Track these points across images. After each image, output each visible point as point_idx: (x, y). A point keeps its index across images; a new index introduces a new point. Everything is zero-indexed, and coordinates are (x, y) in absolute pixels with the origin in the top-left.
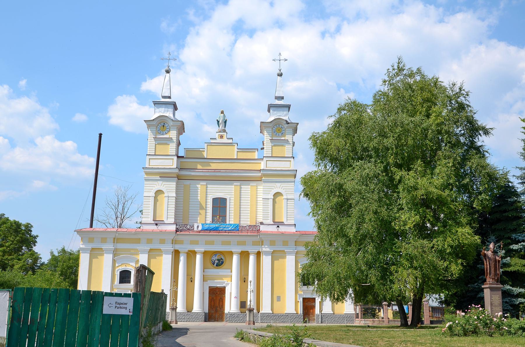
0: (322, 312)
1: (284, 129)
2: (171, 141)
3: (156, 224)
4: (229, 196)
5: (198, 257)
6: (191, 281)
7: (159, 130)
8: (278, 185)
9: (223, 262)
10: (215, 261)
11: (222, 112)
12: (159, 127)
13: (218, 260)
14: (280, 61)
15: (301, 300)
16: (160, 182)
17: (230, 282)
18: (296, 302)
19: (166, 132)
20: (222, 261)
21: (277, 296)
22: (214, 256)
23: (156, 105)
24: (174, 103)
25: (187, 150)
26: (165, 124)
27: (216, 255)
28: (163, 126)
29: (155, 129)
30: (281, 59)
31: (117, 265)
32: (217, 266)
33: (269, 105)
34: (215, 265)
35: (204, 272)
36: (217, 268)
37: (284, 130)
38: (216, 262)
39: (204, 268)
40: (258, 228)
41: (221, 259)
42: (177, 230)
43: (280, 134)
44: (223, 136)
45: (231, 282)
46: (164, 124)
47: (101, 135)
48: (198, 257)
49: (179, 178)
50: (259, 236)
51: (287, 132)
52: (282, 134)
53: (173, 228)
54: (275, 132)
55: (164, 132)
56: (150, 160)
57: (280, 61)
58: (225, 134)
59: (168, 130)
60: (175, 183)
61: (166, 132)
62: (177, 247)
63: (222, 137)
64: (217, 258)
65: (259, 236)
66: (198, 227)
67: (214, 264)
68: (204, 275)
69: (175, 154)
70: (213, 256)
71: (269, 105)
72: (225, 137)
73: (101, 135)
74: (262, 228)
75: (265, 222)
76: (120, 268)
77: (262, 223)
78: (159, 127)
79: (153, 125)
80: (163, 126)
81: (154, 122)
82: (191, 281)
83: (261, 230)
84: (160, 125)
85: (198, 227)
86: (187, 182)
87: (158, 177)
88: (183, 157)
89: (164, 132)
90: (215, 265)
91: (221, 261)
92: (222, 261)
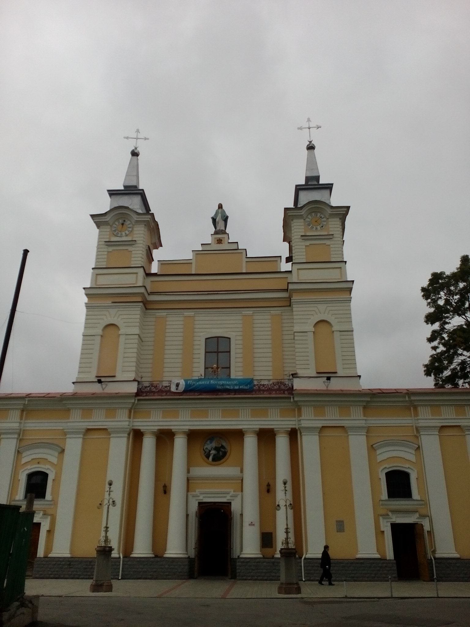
0: (437, 556)
1: (325, 219)
2: (134, 246)
3: (100, 381)
4: (234, 334)
5: (180, 443)
6: (165, 492)
7: (115, 231)
8: (322, 307)
9: (225, 454)
10: (210, 451)
11: (220, 206)
12: (115, 226)
13: (216, 449)
14: (309, 128)
15: (389, 529)
16: (113, 311)
17: (240, 493)
18: (380, 533)
19: (127, 232)
20: (223, 450)
21: (337, 521)
22: (208, 442)
23: (113, 197)
24: (142, 192)
25: (162, 263)
26: (126, 220)
27: (211, 440)
28: (123, 224)
29: (108, 230)
30: (311, 126)
31: (24, 461)
32: (214, 460)
33: (297, 186)
34: (211, 458)
35: (188, 472)
36: (215, 465)
37: (324, 221)
38: (213, 452)
39: (190, 463)
40: (290, 385)
41: (223, 447)
42: (139, 393)
43: (319, 227)
44: (221, 240)
45: (242, 491)
46: (124, 221)
47: (26, 252)
48: (180, 443)
49: (147, 305)
50: (293, 398)
51: (330, 223)
52: (322, 227)
53: (133, 388)
54: (309, 225)
55: (124, 233)
56: (98, 276)
57: (309, 128)
58: (225, 236)
59: (130, 229)
60: (139, 312)
61: (127, 232)
62: (140, 424)
63: (220, 241)
64: (214, 445)
65: (293, 398)
66: (178, 385)
67: (208, 456)
68: (188, 480)
69: (140, 266)
70: (207, 441)
71: (297, 186)
72: (225, 241)
73: (26, 252)
74: (298, 384)
75: (300, 372)
76: (29, 467)
77: (294, 375)
78: (115, 226)
79: (106, 223)
80: (123, 224)
81: (105, 216)
82: (165, 492)
83: (294, 389)
84: (117, 223)
85: (178, 385)
86: (163, 313)
87: (108, 302)
88: (155, 275)
89: (124, 233)
90: (211, 458)
91: (222, 451)
92: (223, 450)
